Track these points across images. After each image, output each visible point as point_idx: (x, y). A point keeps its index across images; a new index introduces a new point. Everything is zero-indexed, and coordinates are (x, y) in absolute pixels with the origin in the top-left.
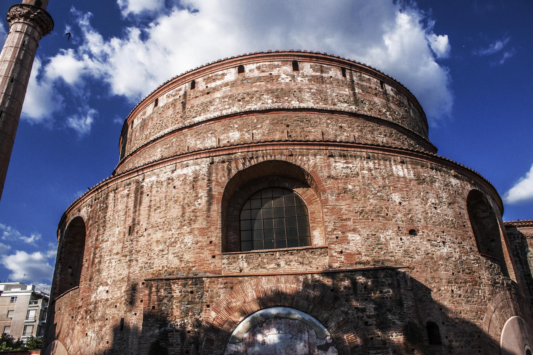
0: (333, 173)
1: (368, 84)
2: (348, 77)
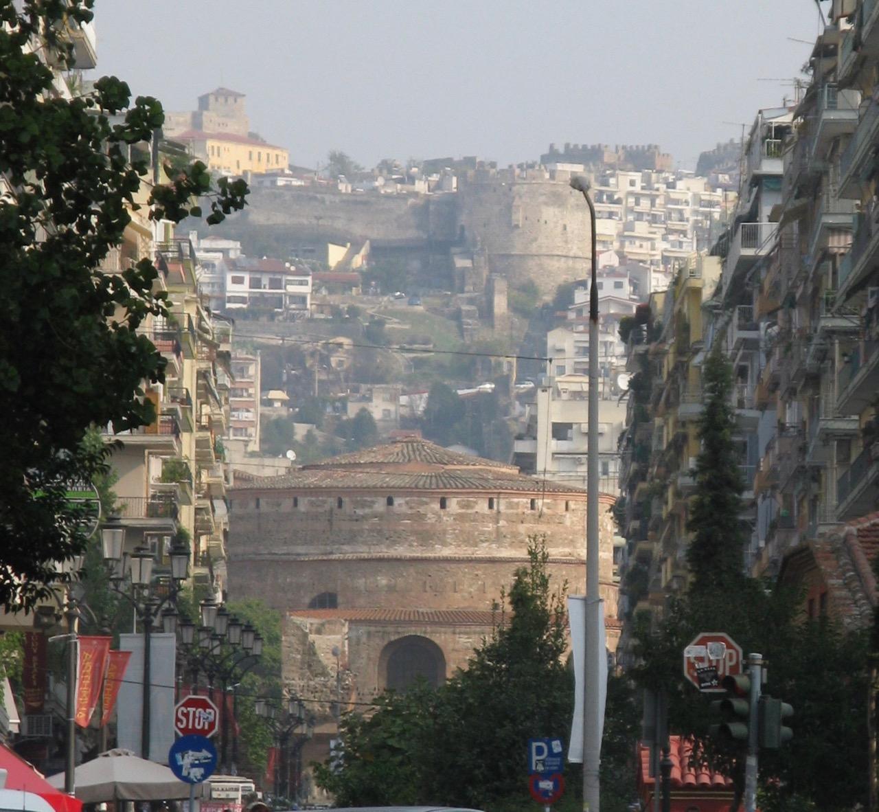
0: (457, 647)
1: (515, 511)
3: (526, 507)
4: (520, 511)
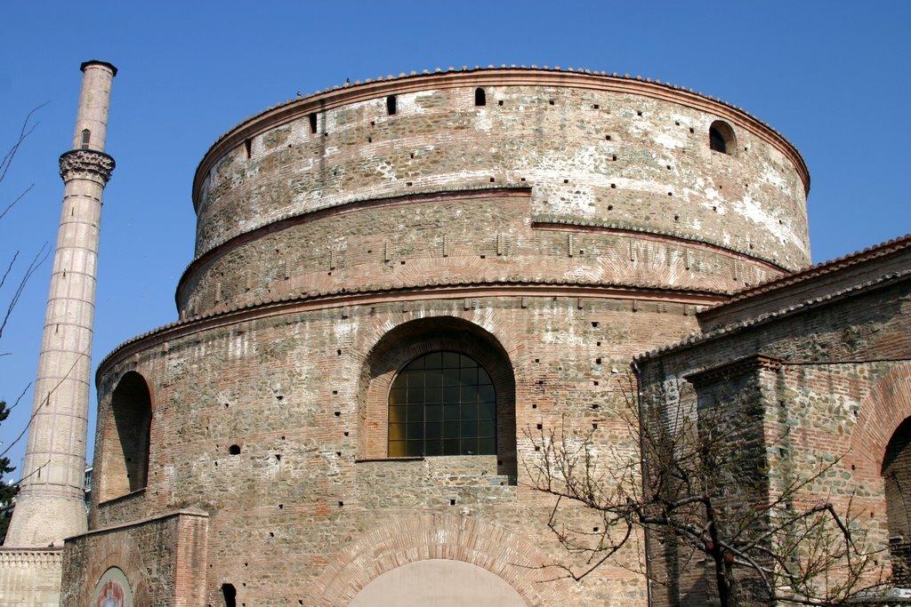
1: (354, 125)
2: (319, 129)
3: (379, 114)
4: (365, 121)
